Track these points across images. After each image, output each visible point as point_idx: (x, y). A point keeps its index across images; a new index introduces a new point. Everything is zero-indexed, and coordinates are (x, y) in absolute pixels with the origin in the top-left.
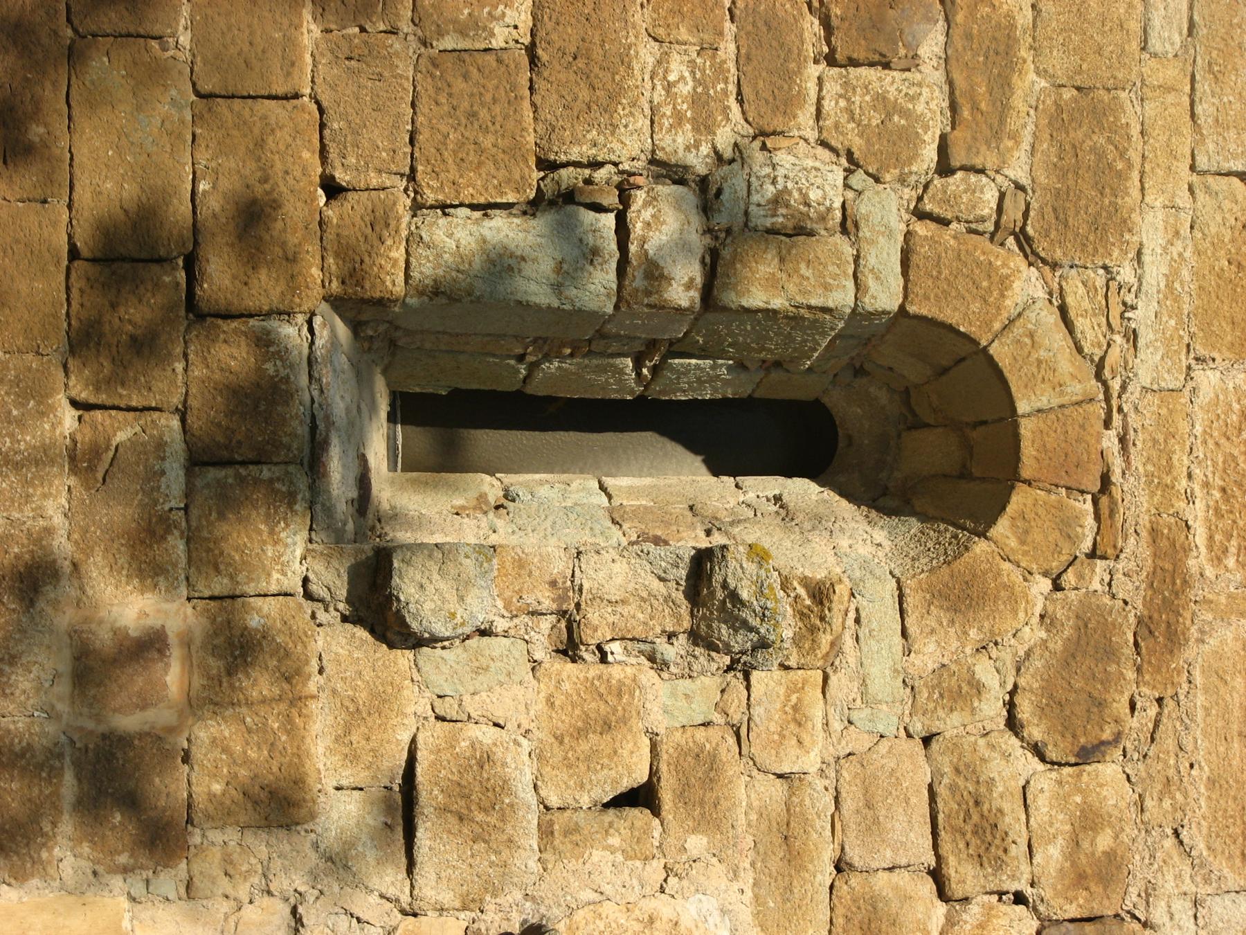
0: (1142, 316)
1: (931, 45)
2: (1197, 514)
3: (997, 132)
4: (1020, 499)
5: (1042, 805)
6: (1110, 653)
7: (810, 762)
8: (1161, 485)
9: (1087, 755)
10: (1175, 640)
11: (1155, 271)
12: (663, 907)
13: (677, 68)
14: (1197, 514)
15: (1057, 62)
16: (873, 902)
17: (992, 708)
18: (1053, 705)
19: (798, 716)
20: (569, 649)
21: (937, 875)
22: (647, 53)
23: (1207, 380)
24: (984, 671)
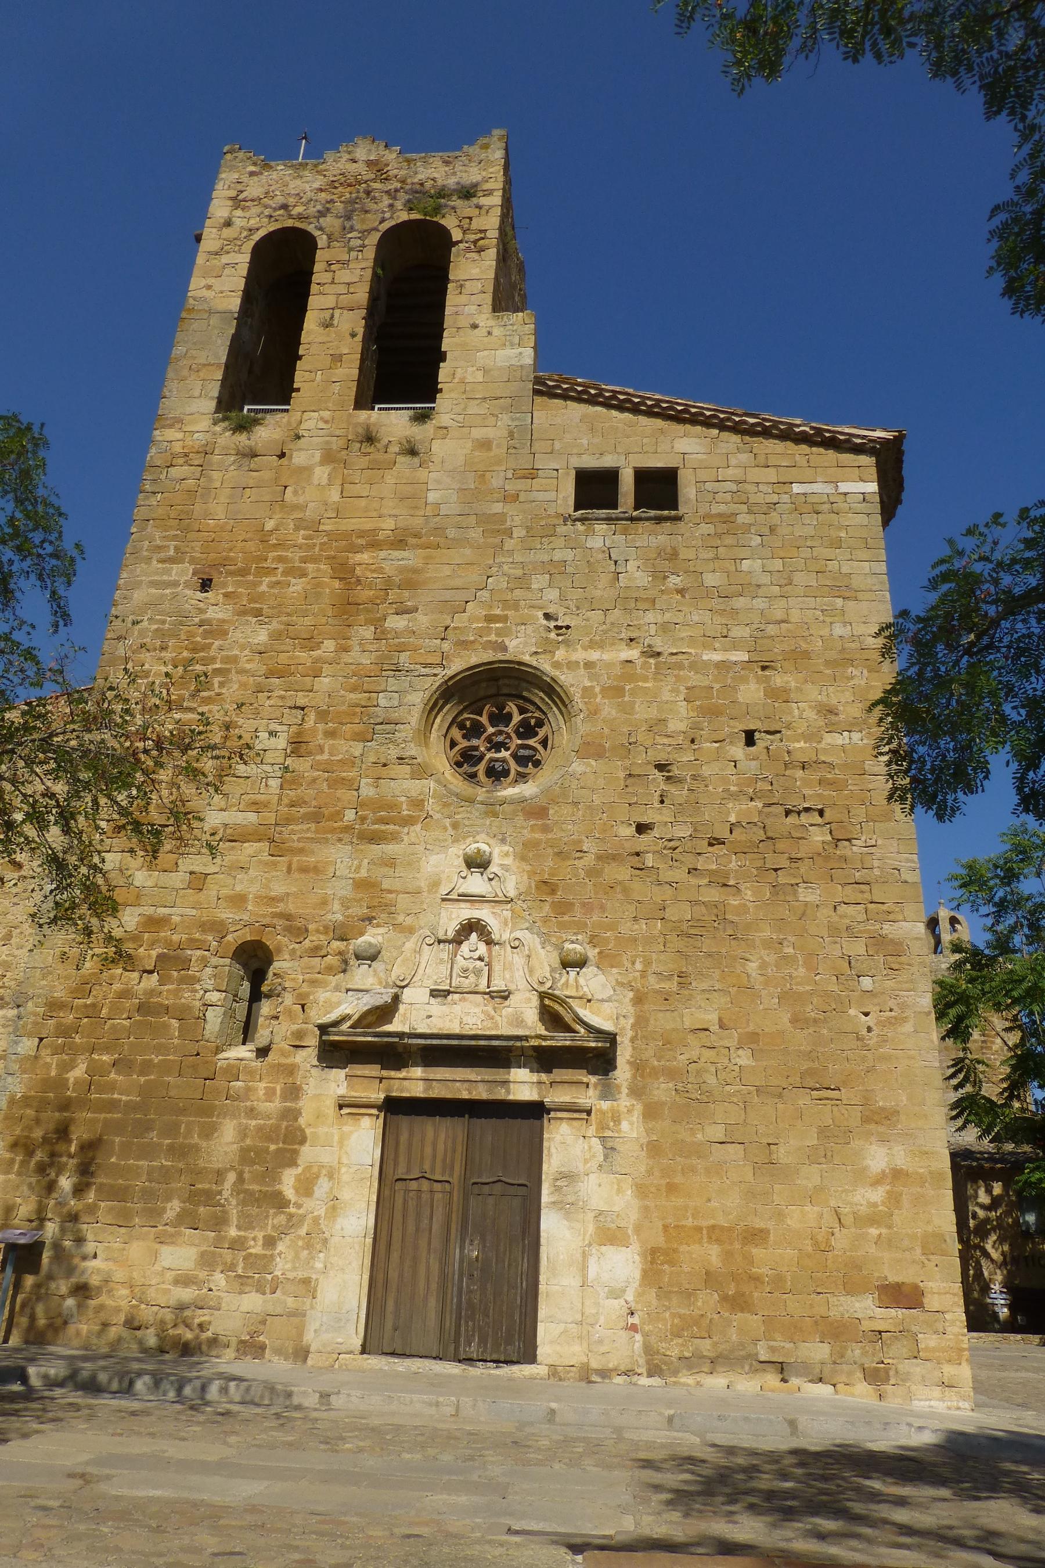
0: (237, 918)
1: (189, 952)
2: (270, 910)
3: (204, 941)
4: (264, 940)
5: (314, 938)
6: (291, 926)
7: (301, 977)
8: (264, 916)
9: (307, 930)
10: (290, 915)
11: (231, 916)
12: (321, 1003)
13: (186, 995)
14: (270, 910)
15: (194, 931)
16: (326, 968)
17: (297, 946)
18: (298, 936)
19: (293, 980)
20: (277, 1018)
21: (323, 957)
22: (183, 1000)
23: (250, 908)
24: (291, 947)
